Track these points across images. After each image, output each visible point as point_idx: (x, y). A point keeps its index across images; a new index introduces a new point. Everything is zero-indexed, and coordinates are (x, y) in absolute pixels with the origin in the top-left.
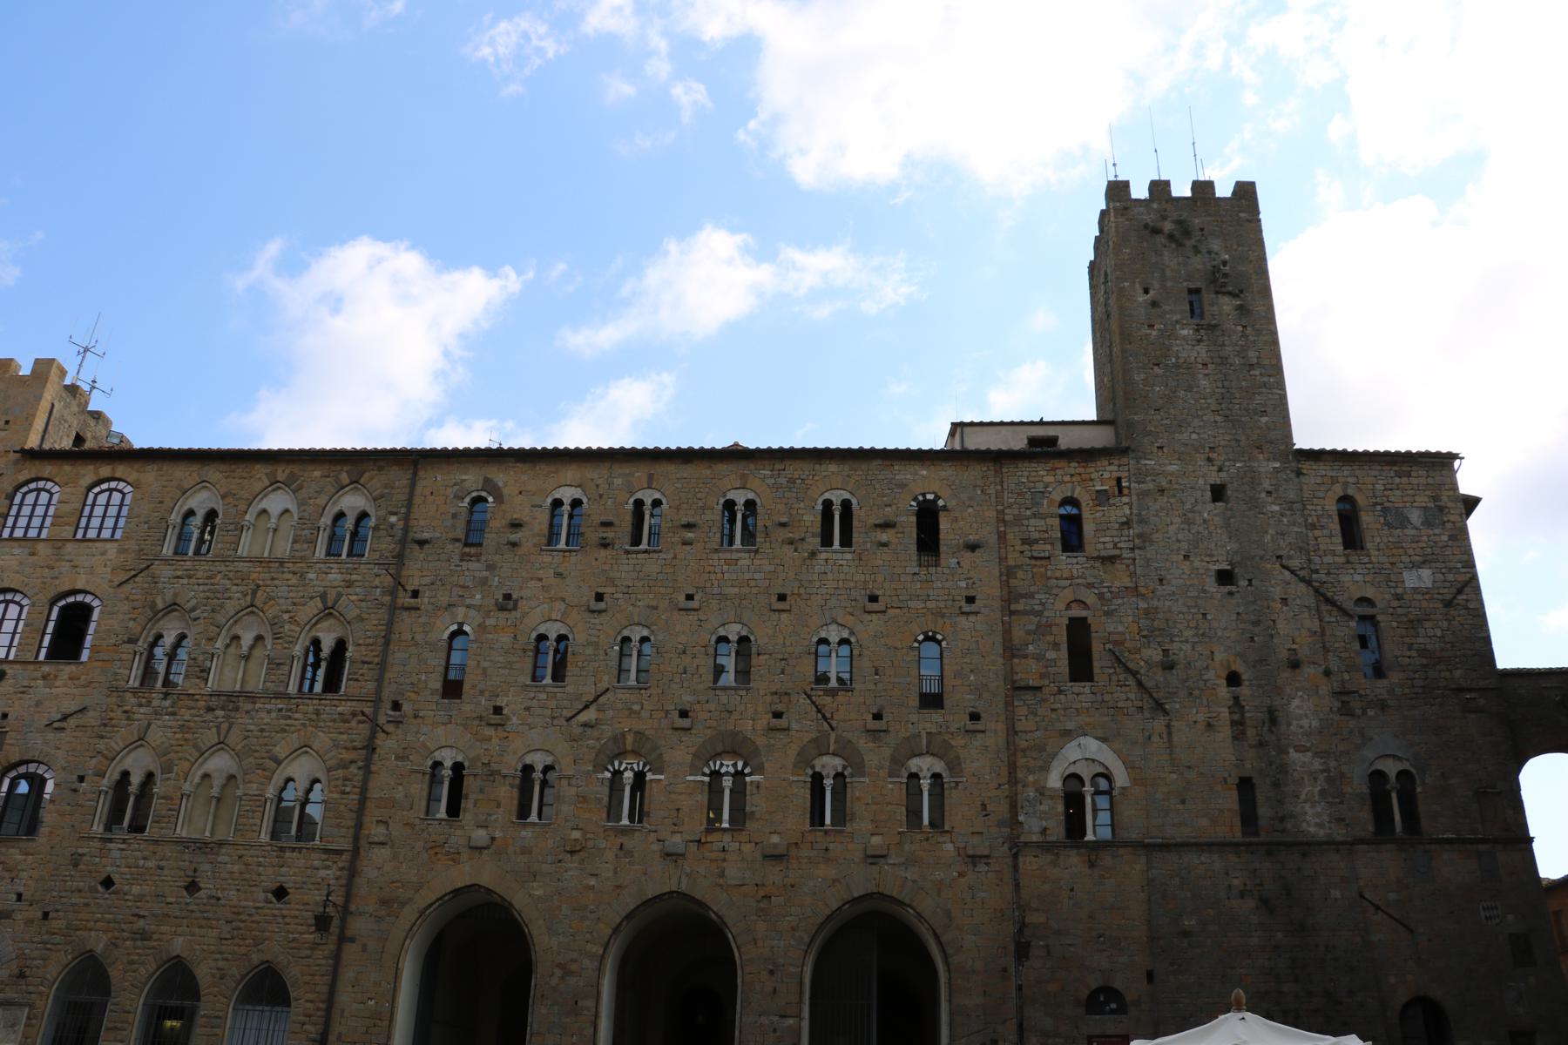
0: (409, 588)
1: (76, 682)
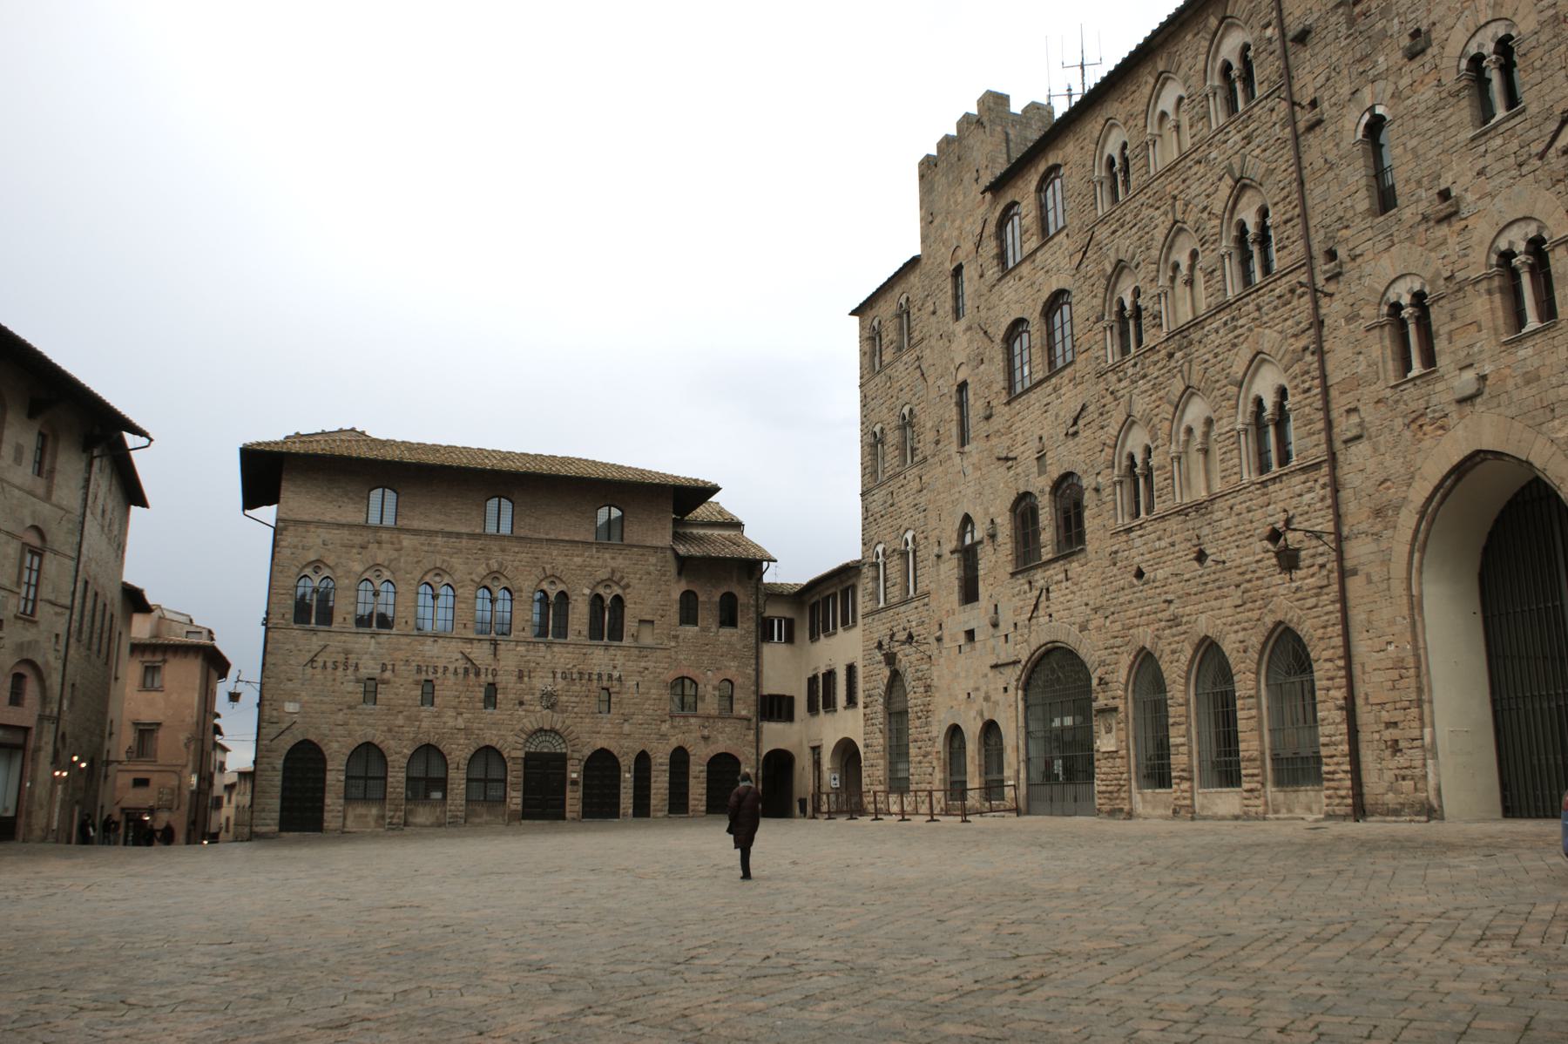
0: (1305, 102)
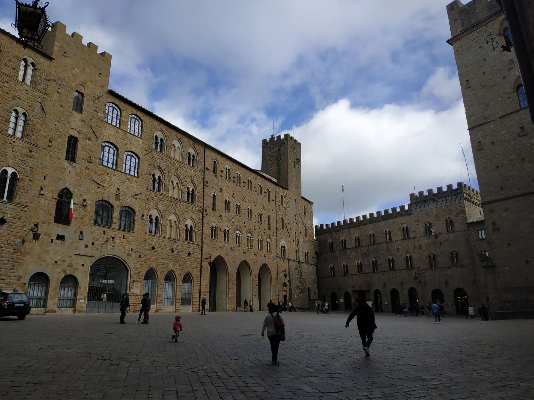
1: (137, 184)
